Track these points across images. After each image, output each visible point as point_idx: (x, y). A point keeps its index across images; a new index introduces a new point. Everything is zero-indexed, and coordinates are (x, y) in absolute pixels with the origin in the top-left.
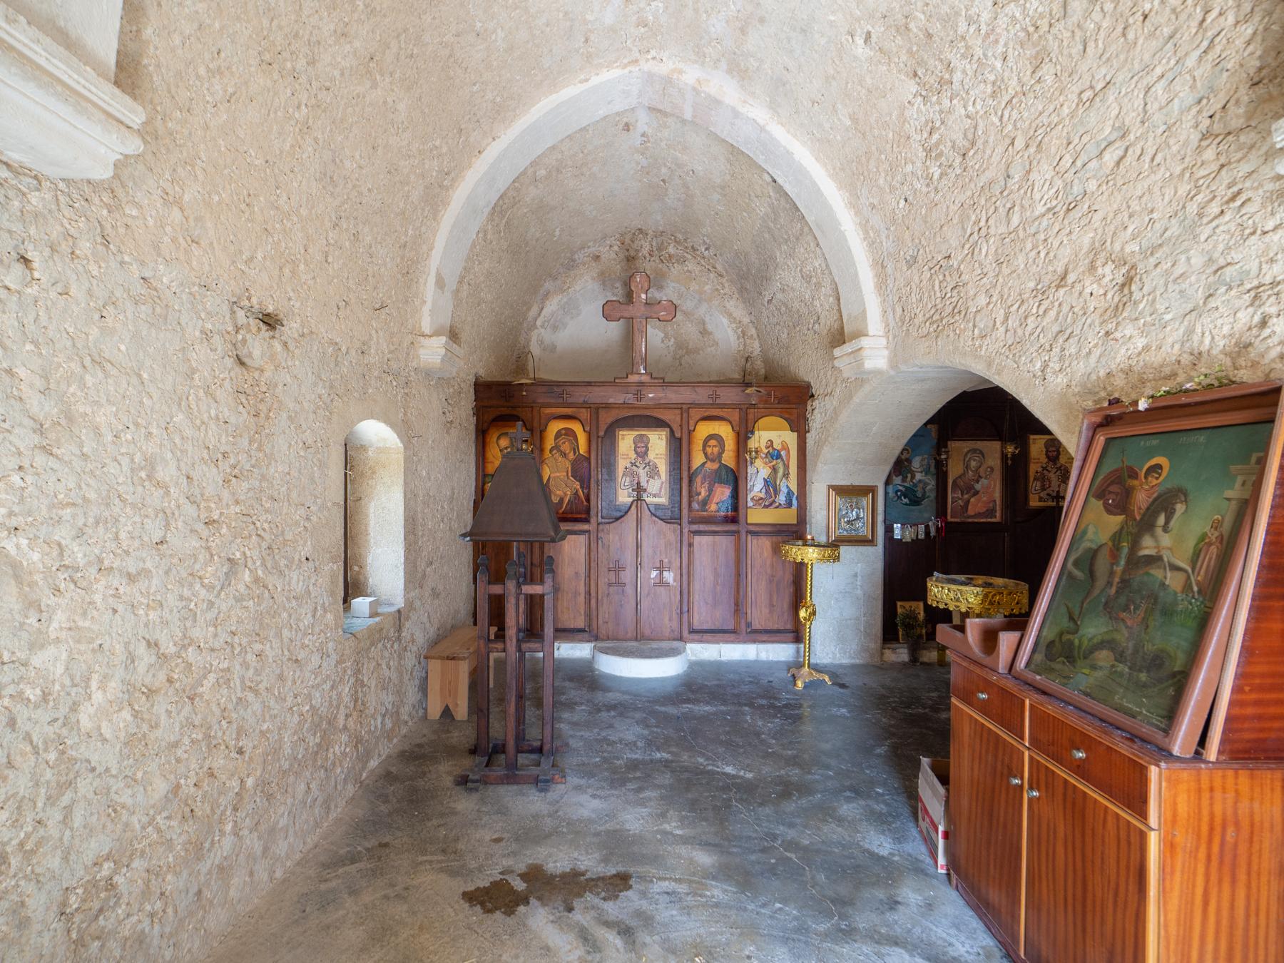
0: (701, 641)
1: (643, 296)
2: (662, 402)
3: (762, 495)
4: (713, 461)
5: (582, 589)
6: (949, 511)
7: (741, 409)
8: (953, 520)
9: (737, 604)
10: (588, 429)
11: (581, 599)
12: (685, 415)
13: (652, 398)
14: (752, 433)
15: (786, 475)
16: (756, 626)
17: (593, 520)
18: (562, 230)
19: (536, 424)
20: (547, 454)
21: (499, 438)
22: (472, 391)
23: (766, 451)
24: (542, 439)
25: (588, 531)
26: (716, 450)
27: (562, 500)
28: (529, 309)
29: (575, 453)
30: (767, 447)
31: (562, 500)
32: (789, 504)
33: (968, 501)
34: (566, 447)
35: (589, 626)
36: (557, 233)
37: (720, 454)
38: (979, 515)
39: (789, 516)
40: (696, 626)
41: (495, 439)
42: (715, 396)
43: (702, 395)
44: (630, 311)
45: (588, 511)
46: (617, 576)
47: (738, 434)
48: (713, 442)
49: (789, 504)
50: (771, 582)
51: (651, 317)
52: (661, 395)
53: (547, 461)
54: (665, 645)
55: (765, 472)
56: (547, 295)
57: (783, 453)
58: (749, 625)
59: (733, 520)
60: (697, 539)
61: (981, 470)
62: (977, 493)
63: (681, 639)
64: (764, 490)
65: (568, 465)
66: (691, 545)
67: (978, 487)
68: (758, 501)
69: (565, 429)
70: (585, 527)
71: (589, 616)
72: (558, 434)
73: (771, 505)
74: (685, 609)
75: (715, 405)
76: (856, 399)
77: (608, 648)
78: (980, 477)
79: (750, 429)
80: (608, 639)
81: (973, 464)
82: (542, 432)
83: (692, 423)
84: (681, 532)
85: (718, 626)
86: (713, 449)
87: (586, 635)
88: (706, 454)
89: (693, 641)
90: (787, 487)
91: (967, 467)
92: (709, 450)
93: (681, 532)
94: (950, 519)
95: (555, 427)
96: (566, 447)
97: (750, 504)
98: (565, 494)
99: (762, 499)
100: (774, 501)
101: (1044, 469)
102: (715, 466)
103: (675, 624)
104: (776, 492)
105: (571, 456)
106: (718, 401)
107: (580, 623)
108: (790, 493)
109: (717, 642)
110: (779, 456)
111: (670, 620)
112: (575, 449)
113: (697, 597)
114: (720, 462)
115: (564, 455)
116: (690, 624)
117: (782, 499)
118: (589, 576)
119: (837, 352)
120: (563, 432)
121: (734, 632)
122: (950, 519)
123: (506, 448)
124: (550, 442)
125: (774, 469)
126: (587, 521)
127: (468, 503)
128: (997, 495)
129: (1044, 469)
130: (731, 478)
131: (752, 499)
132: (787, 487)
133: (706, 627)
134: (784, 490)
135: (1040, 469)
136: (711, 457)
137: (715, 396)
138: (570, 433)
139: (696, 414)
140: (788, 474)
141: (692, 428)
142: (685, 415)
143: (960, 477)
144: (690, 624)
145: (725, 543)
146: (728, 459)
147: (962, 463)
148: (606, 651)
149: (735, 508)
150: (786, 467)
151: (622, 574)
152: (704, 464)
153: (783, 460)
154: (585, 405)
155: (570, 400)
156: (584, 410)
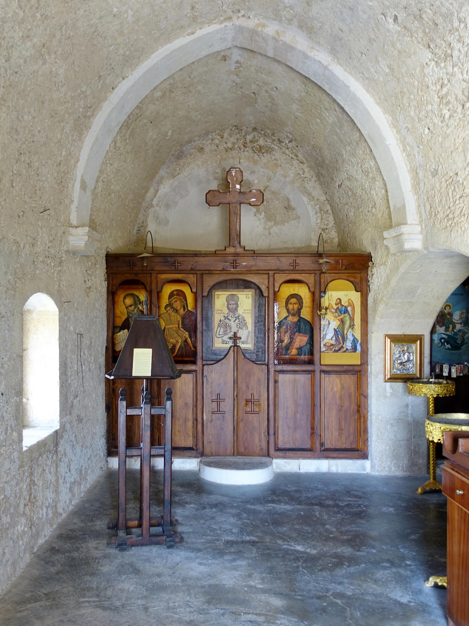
0: (284, 458)
1: (238, 187)
2: (253, 268)
3: (333, 342)
4: (294, 315)
5: (190, 416)
7: (315, 274)
9: (312, 428)
10: (194, 290)
11: (190, 424)
12: (271, 279)
13: (245, 266)
14: (325, 292)
15: (352, 326)
16: (328, 445)
17: (199, 362)
18: (174, 131)
19: (154, 287)
20: (163, 310)
21: (125, 298)
22: (104, 261)
23: (335, 307)
24: (159, 298)
25: (195, 371)
26: (296, 307)
27: (174, 346)
28: (146, 192)
29: (184, 309)
30: (336, 304)
31: (174, 346)
32: (354, 349)
34: (177, 305)
35: (196, 445)
36: (170, 133)
37: (299, 310)
39: (355, 359)
40: (281, 445)
41: (122, 299)
42: (295, 264)
43: (285, 262)
44: (229, 198)
45: (195, 354)
46: (218, 406)
47: (313, 294)
48: (294, 300)
49: (354, 349)
50: (340, 410)
51: (243, 203)
52: (252, 263)
53: (163, 316)
54: (256, 459)
55: (335, 324)
56: (160, 182)
57: (349, 309)
58: (322, 445)
59: (311, 362)
60: (281, 377)
63: (268, 455)
64: (334, 338)
65: (179, 319)
66: (276, 382)
68: (330, 347)
69: (177, 290)
70: (193, 367)
71: (196, 437)
72: (171, 295)
73: (340, 349)
74: (272, 432)
75: (294, 271)
76: (402, 270)
77: (212, 462)
79: (323, 289)
80: (212, 455)
82: (159, 293)
83: (277, 285)
84: (268, 371)
85: (298, 446)
86: (293, 306)
87: (194, 452)
88: (288, 310)
89: (278, 457)
90: (353, 335)
92: (290, 307)
93: (268, 371)
95: (168, 289)
96: (177, 305)
97: (323, 349)
98: (177, 342)
99: (332, 345)
100: (342, 347)
102: (296, 319)
103: (264, 445)
104: (344, 339)
105: (182, 312)
106: (297, 268)
107: (189, 443)
108: (355, 341)
109: (298, 458)
110: (346, 311)
111: (260, 440)
112: (185, 307)
113: (281, 423)
114: (299, 315)
115: (176, 311)
116: (276, 444)
117: (348, 345)
118: (196, 406)
119: (386, 234)
120: (175, 293)
121: (311, 450)
123: (131, 306)
124: (165, 301)
125: (342, 321)
126: (194, 362)
127: (102, 349)
130: (308, 327)
131: (325, 345)
132: (353, 335)
133: (288, 446)
134: (350, 338)
136: (292, 312)
137: (295, 264)
138: (181, 294)
139: (280, 278)
140: (354, 325)
141: (276, 289)
142: (271, 279)
144: (276, 444)
145: (303, 379)
146: (306, 313)
148: (209, 464)
149: (311, 353)
150: (352, 319)
151: (222, 404)
152: (286, 318)
153: (349, 314)
154: (192, 271)
155: (180, 268)
156: (191, 275)
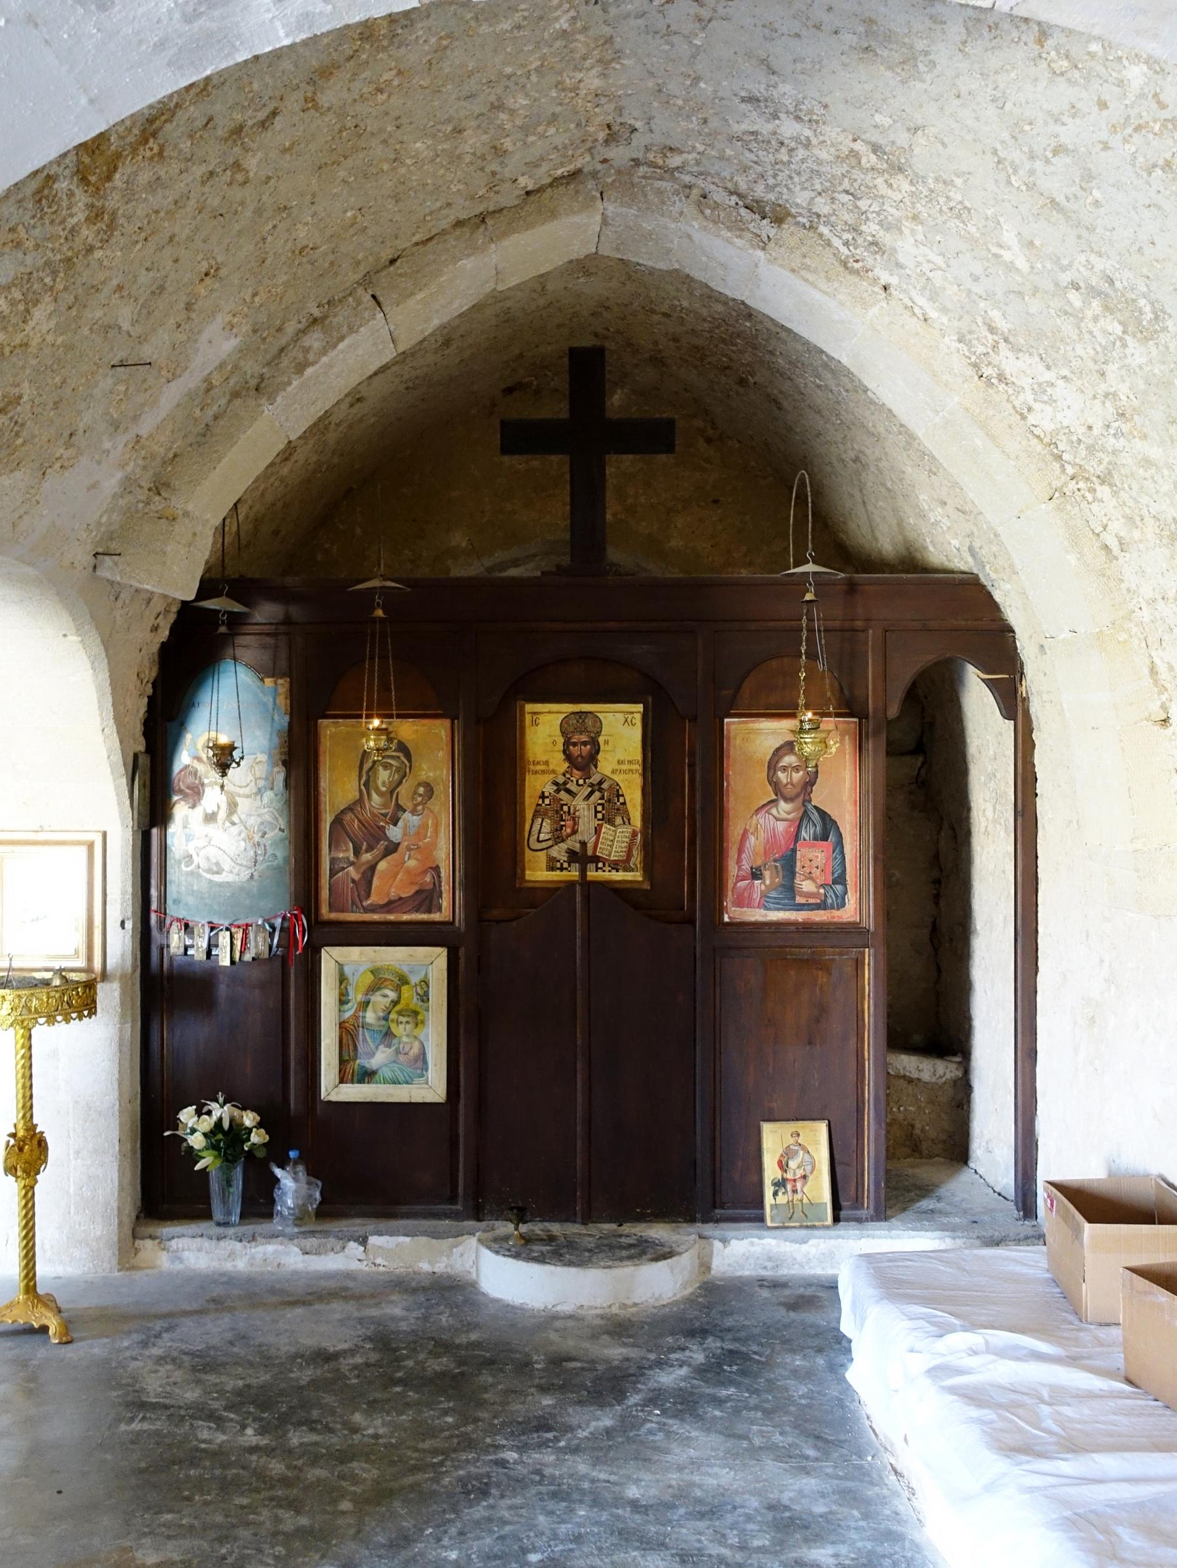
6: (325, 894)
8: (334, 916)
33: (373, 868)
38: (389, 906)
61: (404, 790)
62: (392, 848)
67: (394, 833)
78: (400, 808)
81: (383, 775)
91: (368, 784)
94: (325, 913)
101: (560, 787)
122: (325, 913)
128: (443, 850)
129: (560, 787)
135: (549, 789)
143: (350, 809)
147: (355, 774)
